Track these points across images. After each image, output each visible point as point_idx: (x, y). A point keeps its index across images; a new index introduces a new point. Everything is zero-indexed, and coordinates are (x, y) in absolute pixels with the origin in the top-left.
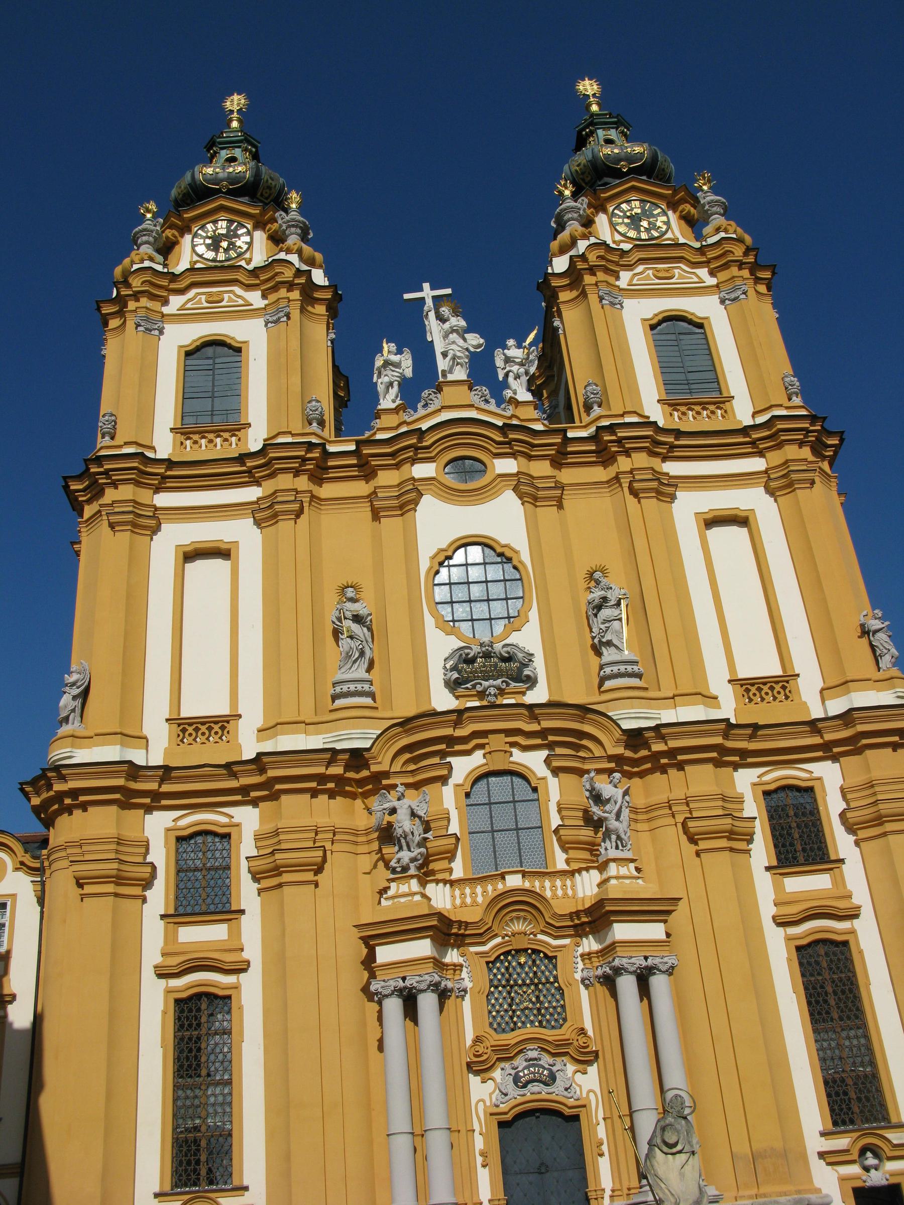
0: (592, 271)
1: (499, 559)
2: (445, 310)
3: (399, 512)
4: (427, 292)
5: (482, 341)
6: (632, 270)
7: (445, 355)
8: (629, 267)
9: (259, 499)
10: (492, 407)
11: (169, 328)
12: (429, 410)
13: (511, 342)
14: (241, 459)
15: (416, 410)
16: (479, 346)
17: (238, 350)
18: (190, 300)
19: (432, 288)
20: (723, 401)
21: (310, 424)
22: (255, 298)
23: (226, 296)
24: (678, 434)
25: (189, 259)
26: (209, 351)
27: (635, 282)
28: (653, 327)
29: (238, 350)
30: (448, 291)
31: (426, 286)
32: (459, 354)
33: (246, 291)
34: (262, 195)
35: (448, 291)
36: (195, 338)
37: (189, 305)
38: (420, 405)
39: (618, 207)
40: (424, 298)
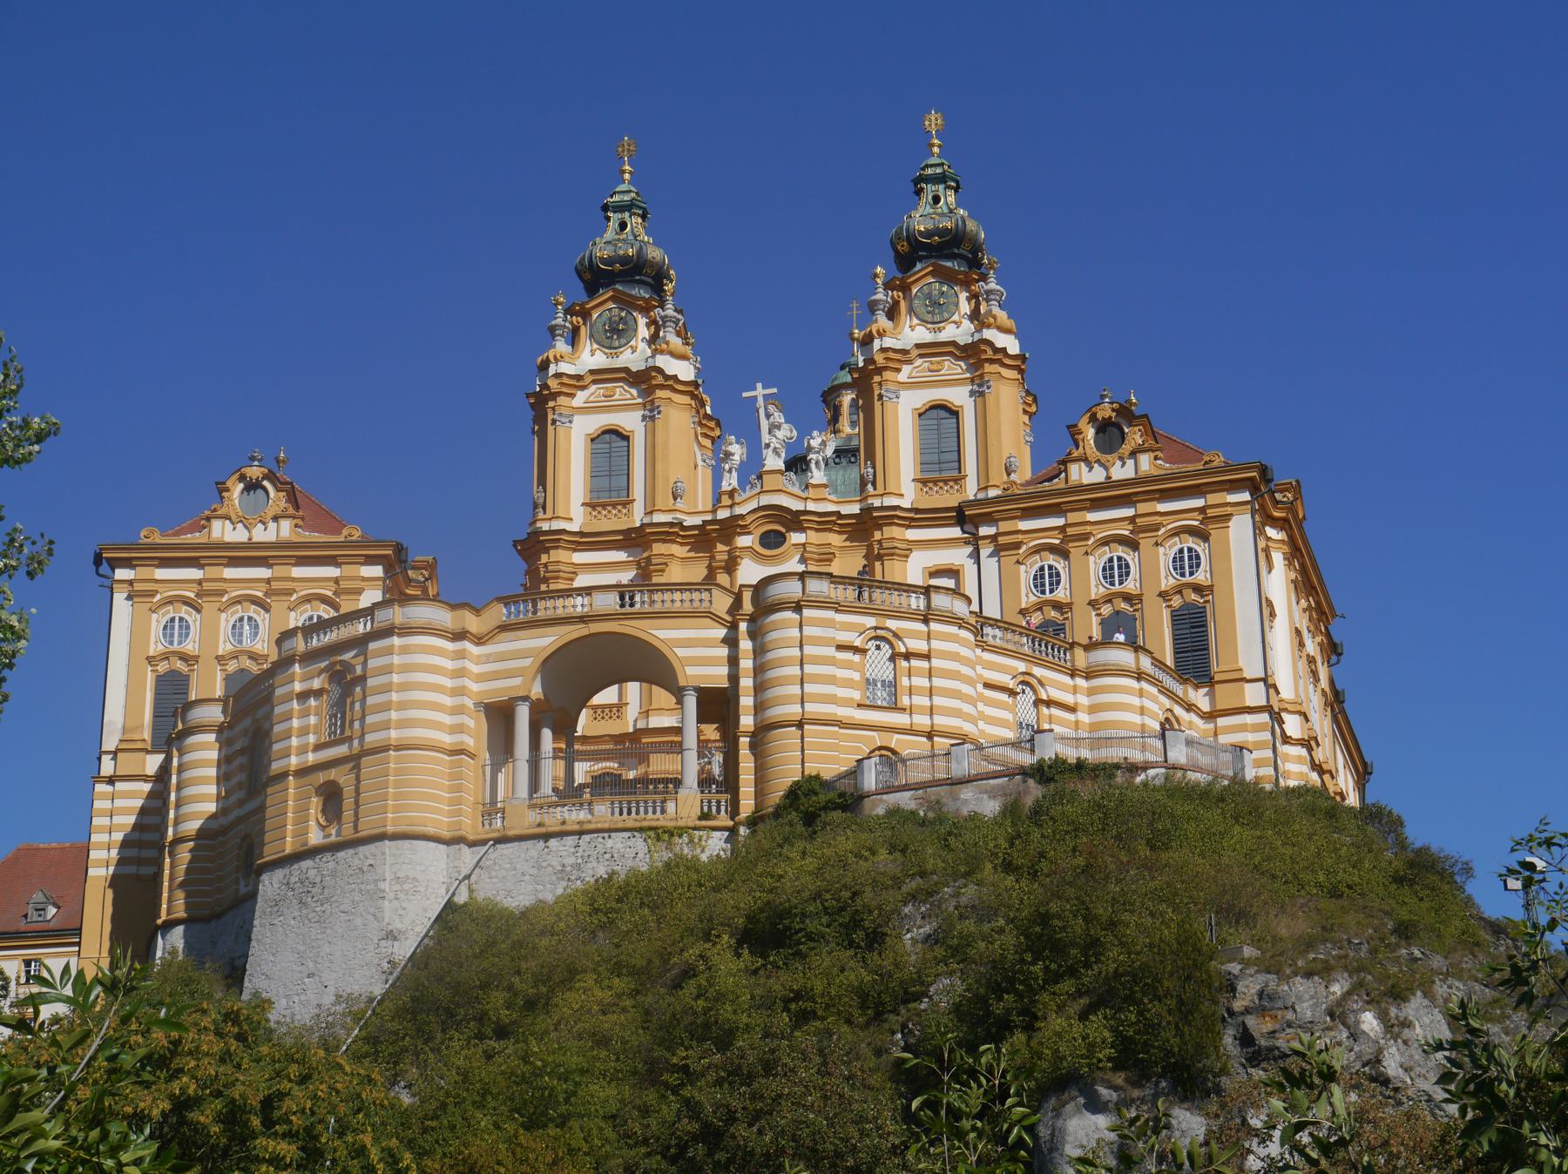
0: (879, 371)
4: (760, 391)
5: (795, 433)
7: (768, 446)
8: (910, 362)
10: (796, 490)
11: (576, 418)
14: (630, 530)
15: (744, 491)
16: (791, 438)
17: (626, 438)
18: (593, 394)
19: (764, 388)
20: (959, 479)
21: (675, 499)
23: (618, 390)
24: (917, 511)
26: (607, 437)
27: (913, 375)
28: (920, 415)
29: (626, 438)
30: (775, 390)
31: (759, 386)
32: (778, 446)
35: (775, 390)
37: (591, 399)
38: (747, 488)
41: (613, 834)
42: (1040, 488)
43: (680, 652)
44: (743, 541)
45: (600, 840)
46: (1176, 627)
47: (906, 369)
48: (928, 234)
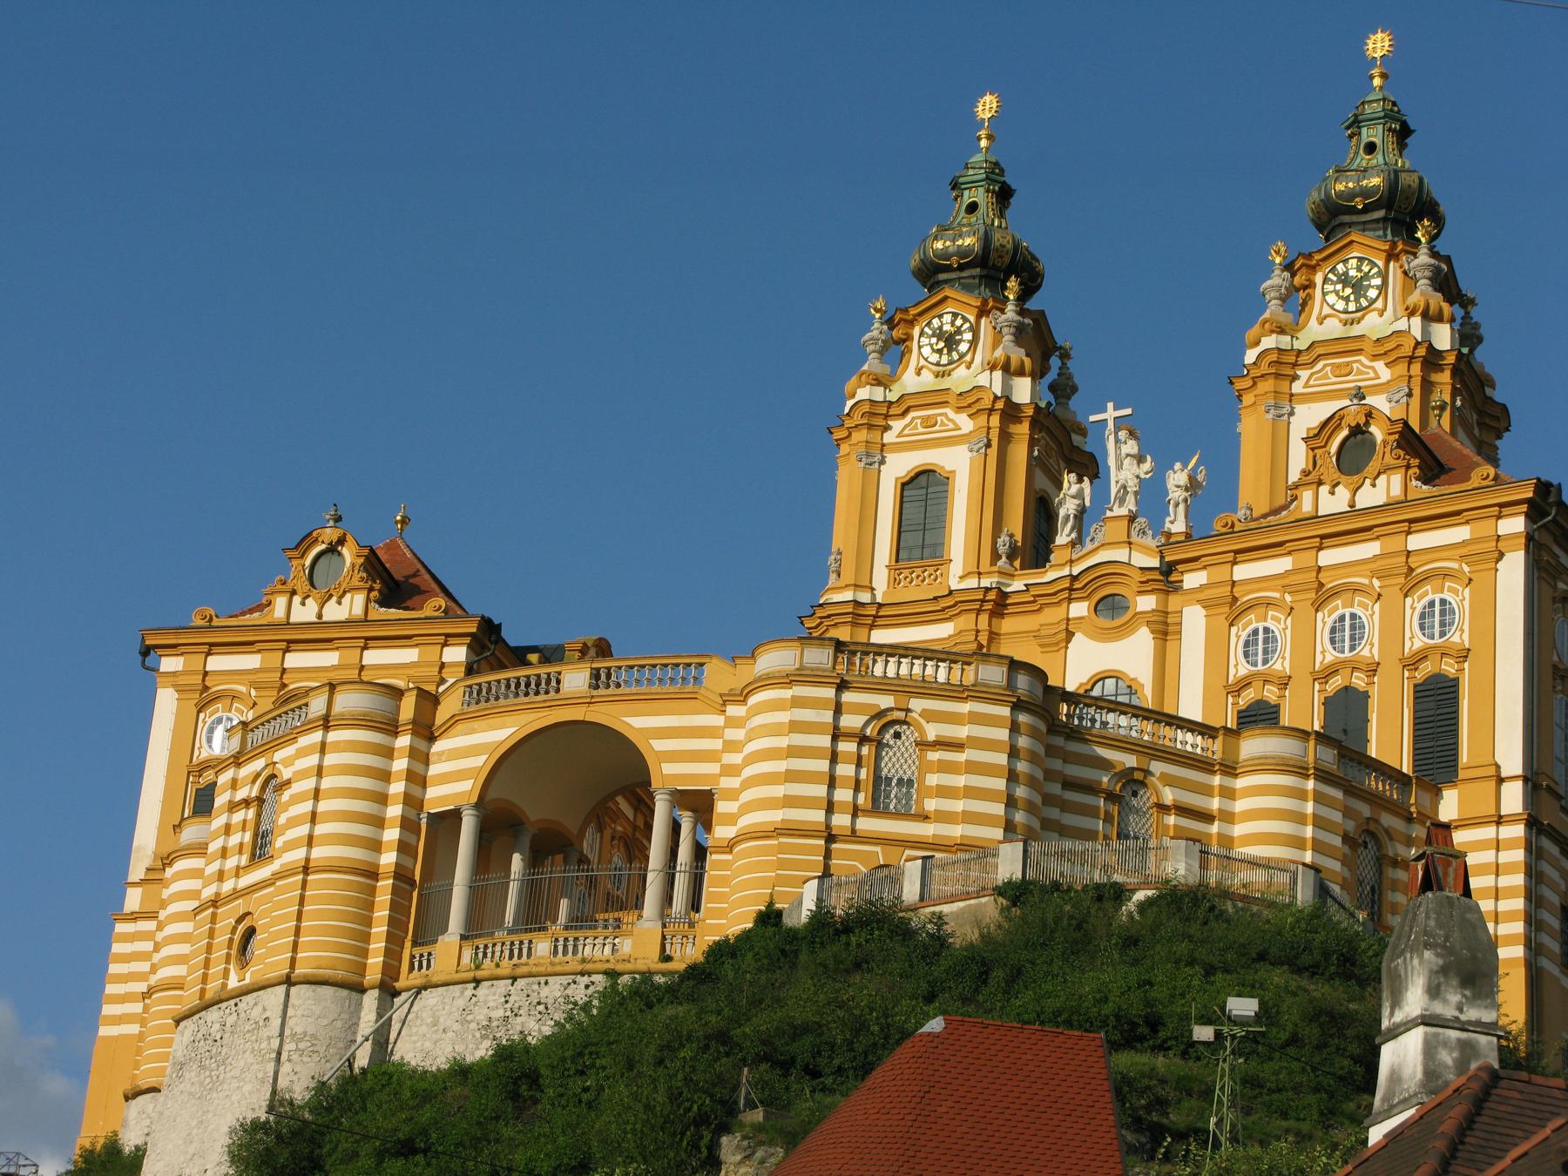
1: (1128, 691)
2: (1123, 434)
3: (1056, 648)
6: (1312, 368)
9: (950, 636)
12: (1096, 544)
13: (1178, 466)
14: (935, 598)
22: (966, 423)
25: (915, 363)
26: (923, 478)
30: (1128, 411)
31: (1110, 405)
33: (957, 412)
34: (994, 265)
35: (1128, 411)
36: (910, 468)
37: (906, 432)
39: (1333, 270)
40: (1106, 420)
41: (550, 979)
42: (1264, 522)
43: (659, 745)
44: (1079, 609)
45: (536, 987)
46: (1419, 707)
47: (1304, 374)
48: (1351, 195)
